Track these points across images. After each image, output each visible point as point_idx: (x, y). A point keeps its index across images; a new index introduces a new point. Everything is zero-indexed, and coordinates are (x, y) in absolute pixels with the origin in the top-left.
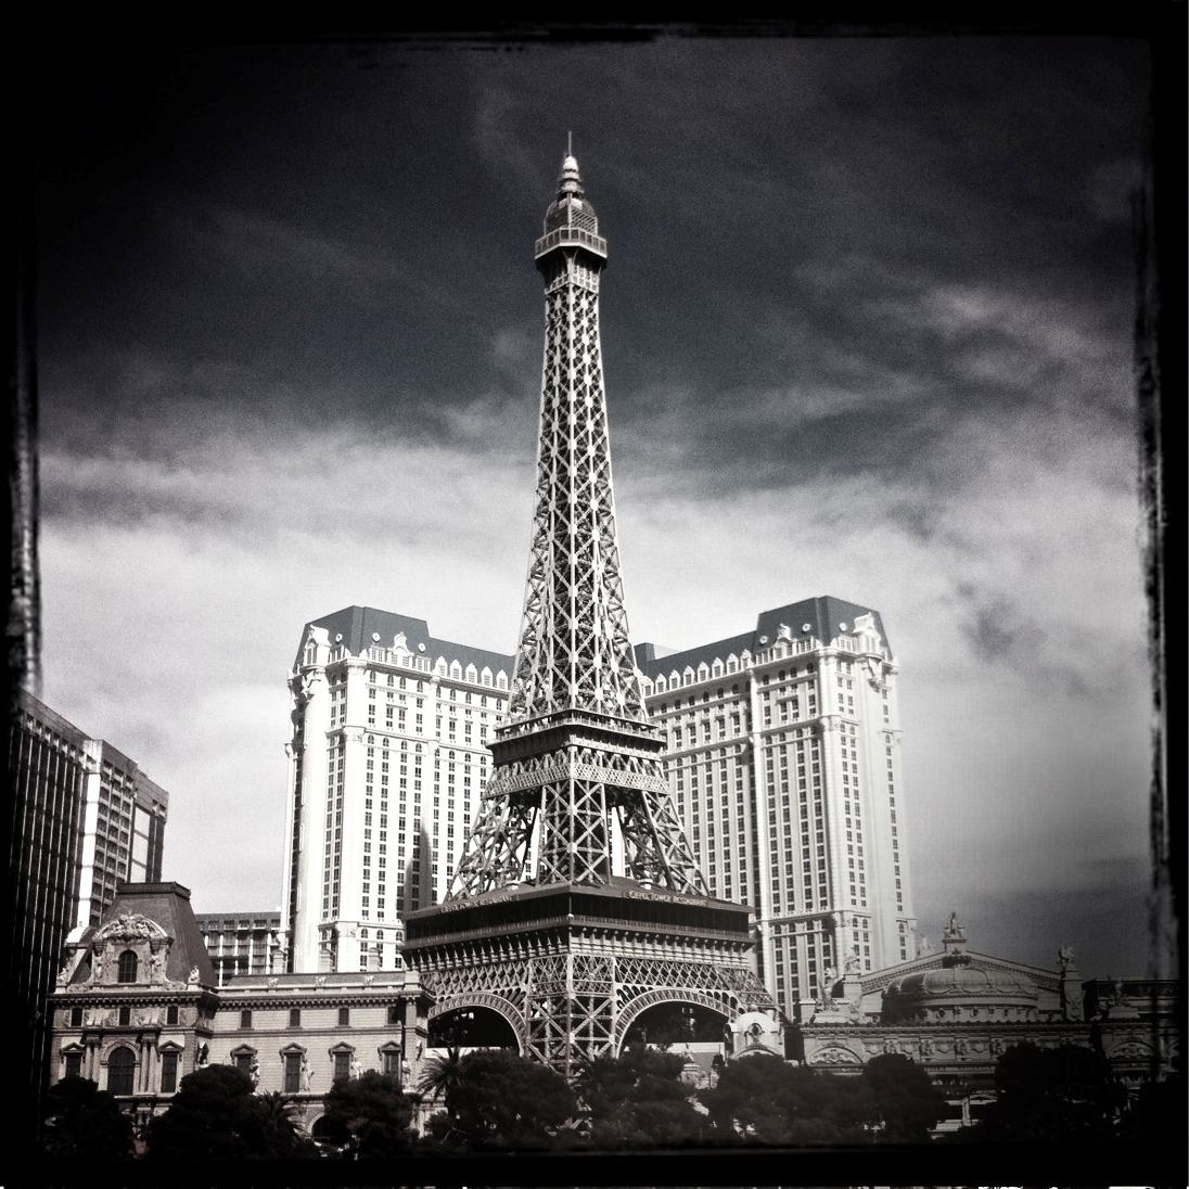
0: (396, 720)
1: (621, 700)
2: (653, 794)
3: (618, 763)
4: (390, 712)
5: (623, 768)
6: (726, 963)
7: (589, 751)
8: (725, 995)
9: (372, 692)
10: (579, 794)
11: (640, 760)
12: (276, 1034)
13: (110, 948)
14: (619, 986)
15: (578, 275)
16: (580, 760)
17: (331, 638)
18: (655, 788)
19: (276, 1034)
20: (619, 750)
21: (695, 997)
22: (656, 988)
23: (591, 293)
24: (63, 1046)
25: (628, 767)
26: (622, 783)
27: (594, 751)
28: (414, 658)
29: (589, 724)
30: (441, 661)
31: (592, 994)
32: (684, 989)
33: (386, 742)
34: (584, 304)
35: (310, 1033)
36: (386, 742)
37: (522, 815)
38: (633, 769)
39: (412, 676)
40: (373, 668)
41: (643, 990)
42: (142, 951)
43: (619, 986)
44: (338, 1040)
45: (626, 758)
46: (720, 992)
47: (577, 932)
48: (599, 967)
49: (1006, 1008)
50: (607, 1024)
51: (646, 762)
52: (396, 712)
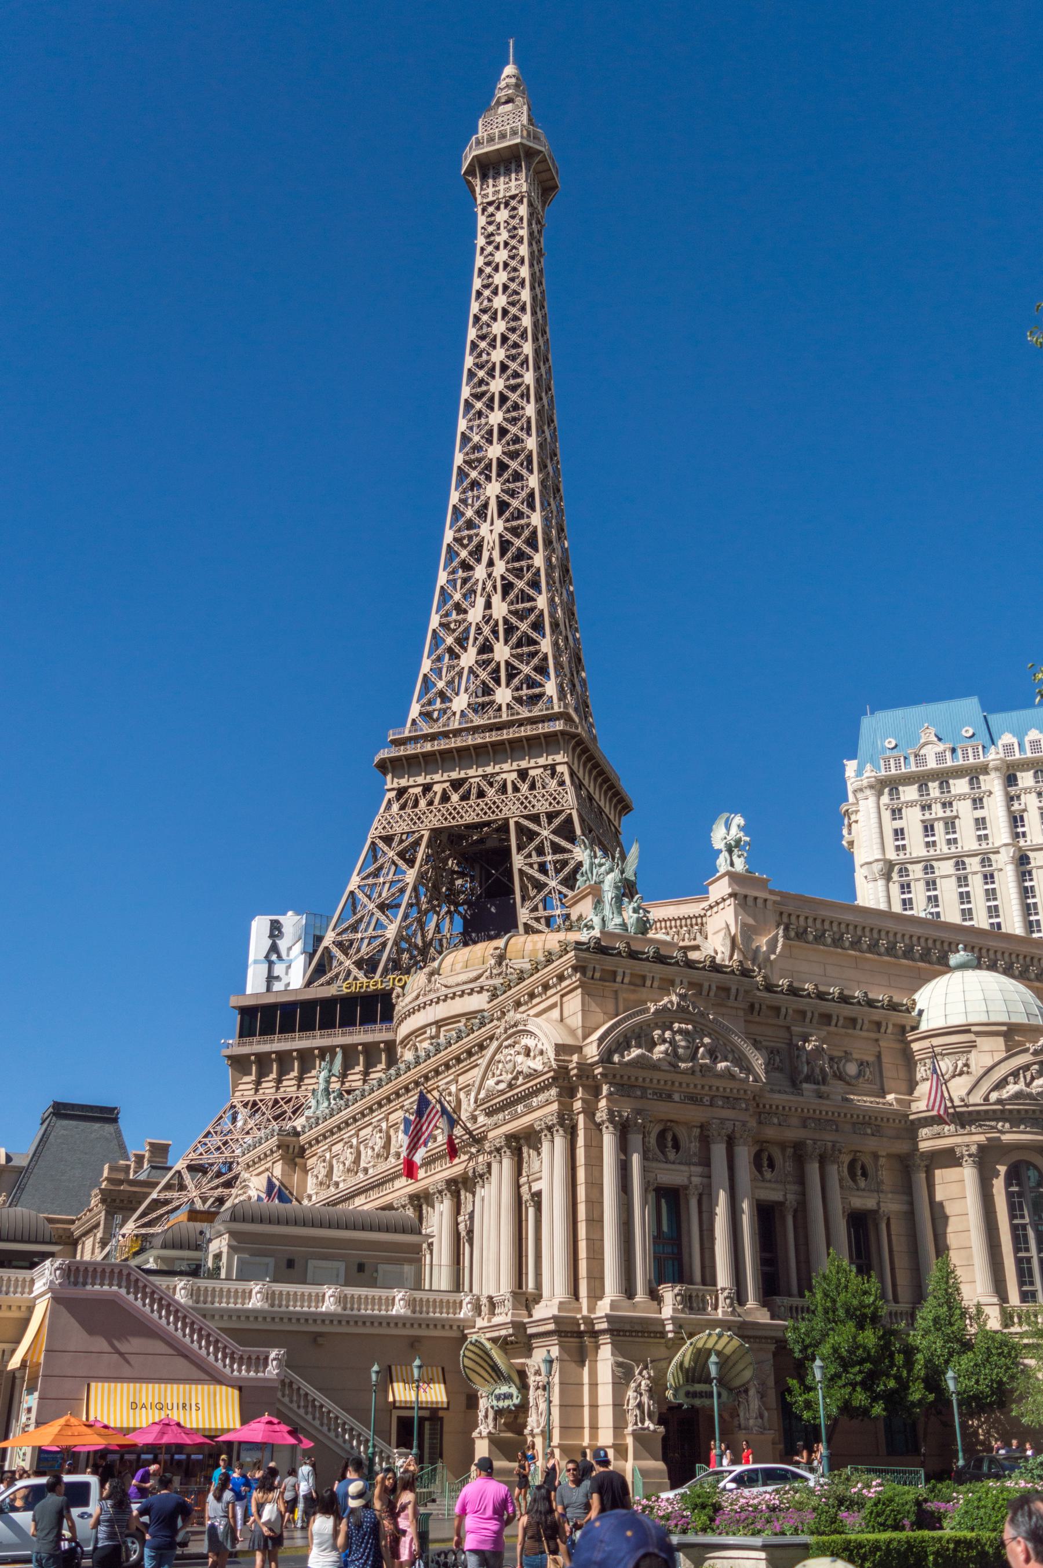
2: (535, 818)
3: (474, 791)
4: (928, 828)
5: (481, 794)
7: (419, 789)
9: (896, 813)
11: (523, 774)
15: (490, 190)
18: (542, 807)
20: (474, 773)
23: (513, 197)
26: (470, 818)
27: (427, 788)
33: (929, 869)
36: (929, 869)
39: (958, 773)
40: (889, 785)
52: (939, 827)
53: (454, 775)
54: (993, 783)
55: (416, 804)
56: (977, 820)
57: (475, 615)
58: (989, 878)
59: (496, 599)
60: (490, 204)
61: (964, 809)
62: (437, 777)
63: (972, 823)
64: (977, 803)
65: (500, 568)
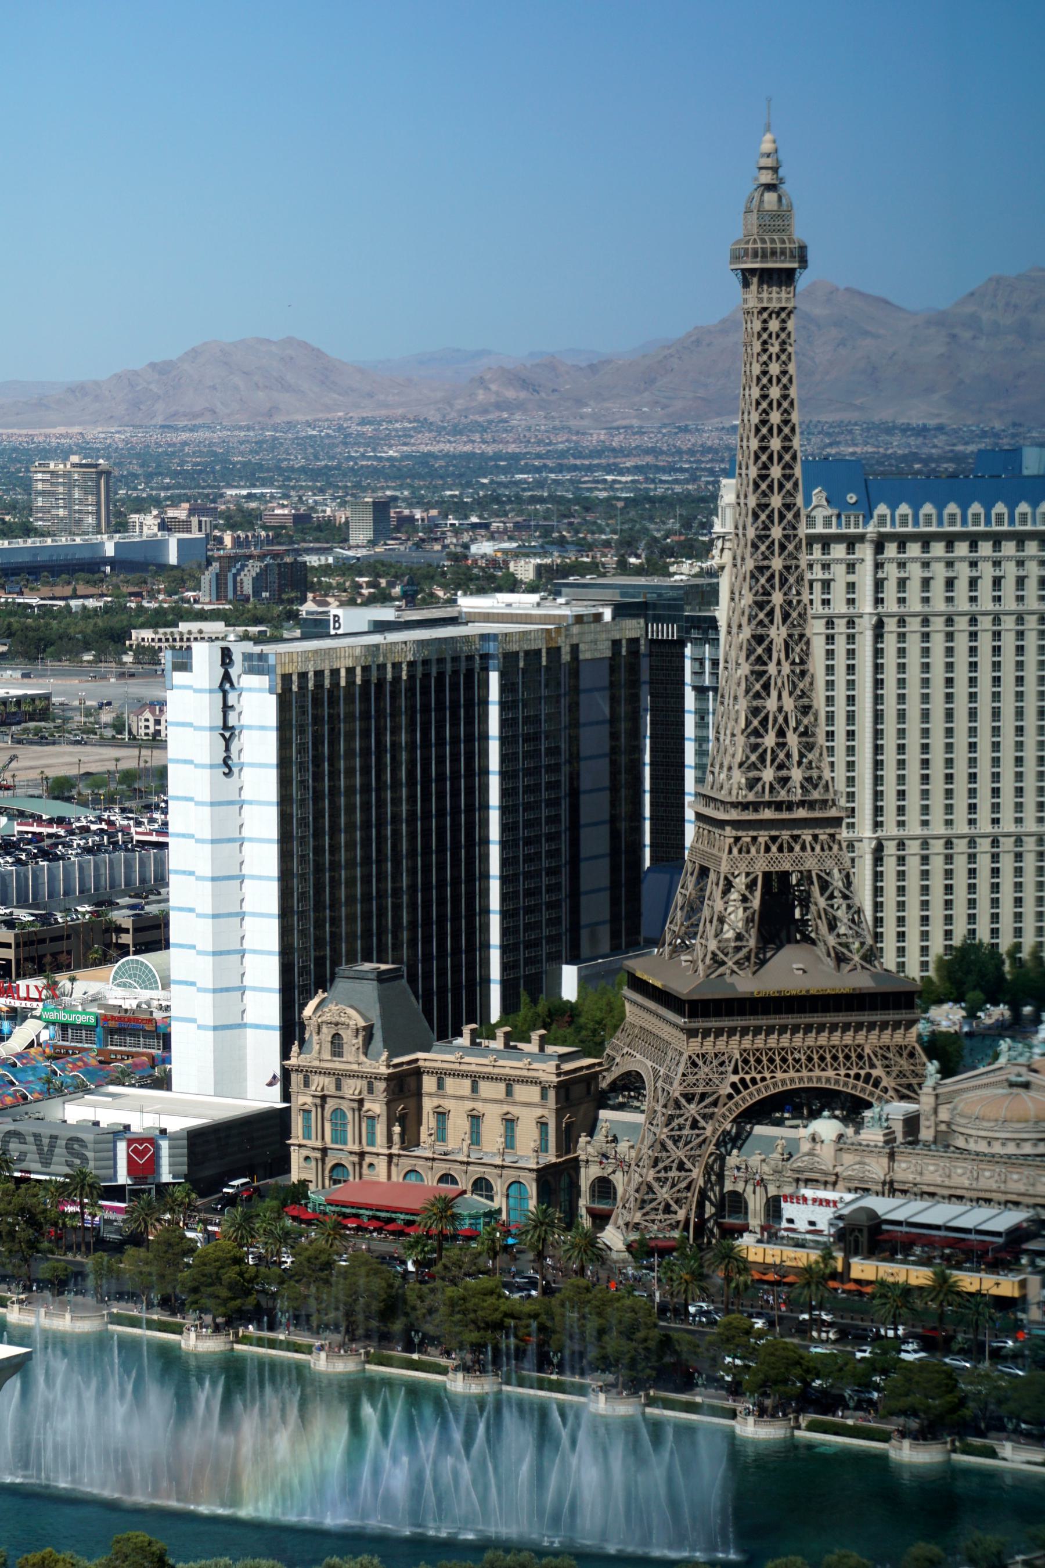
3: (785, 845)
5: (791, 849)
8: (868, 1076)
11: (815, 837)
12: (462, 1098)
13: (324, 1029)
16: (735, 851)
19: (462, 1098)
20: (785, 835)
21: (828, 1080)
22: (779, 1075)
24: (300, 1102)
25: (797, 848)
27: (754, 839)
28: (839, 516)
32: (817, 1072)
34: (774, 325)
35: (485, 1100)
38: (803, 848)
41: (763, 1079)
42: (347, 1035)
43: (735, 1078)
44: (506, 1108)
46: (863, 1072)
48: (715, 1063)
49: (1019, 1142)
51: (821, 837)
53: (774, 833)
54: (866, 552)
55: (748, 852)
56: (848, 584)
57: (771, 704)
58: (851, 638)
59: (785, 694)
60: (765, 309)
61: (839, 572)
62: (761, 833)
63: (844, 586)
64: (851, 567)
65: (786, 668)
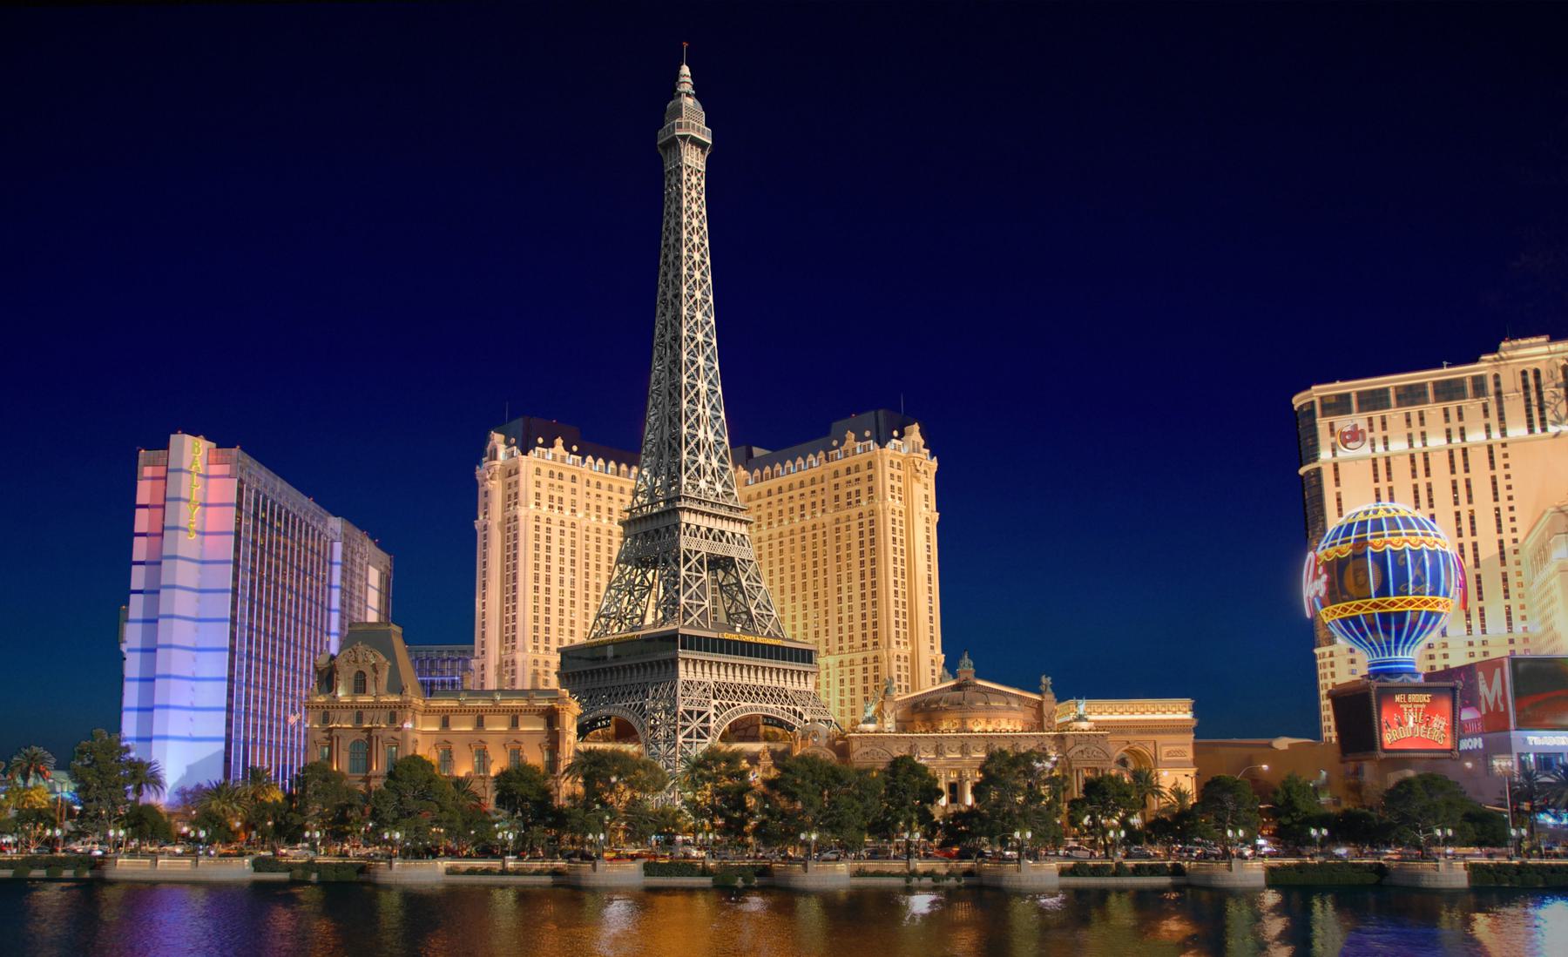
0: (556, 504)
1: (719, 488)
4: (551, 498)
6: (796, 686)
8: (795, 712)
10: (687, 560)
14: (715, 702)
17: (507, 442)
20: (718, 525)
22: (743, 704)
26: (719, 552)
29: (695, 506)
30: (589, 459)
31: (696, 708)
37: (644, 574)
43: (715, 702)
45: (723, 533)
47: (687, 661)
50: (707, 730)
